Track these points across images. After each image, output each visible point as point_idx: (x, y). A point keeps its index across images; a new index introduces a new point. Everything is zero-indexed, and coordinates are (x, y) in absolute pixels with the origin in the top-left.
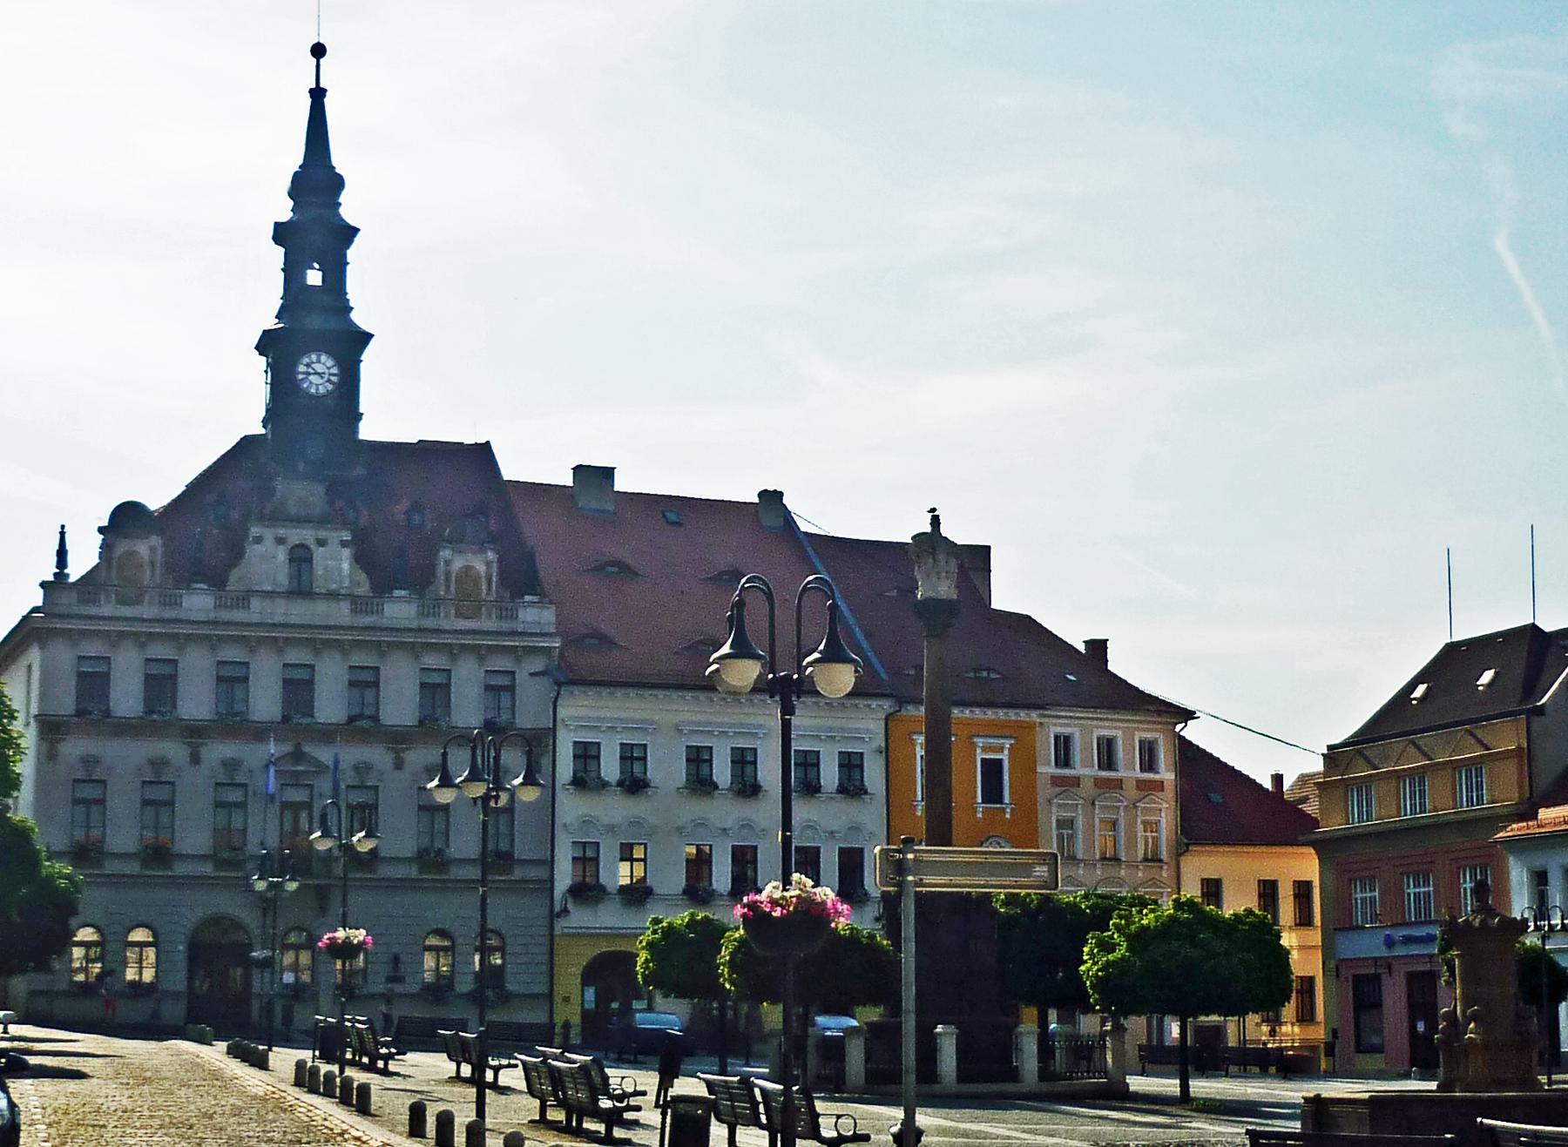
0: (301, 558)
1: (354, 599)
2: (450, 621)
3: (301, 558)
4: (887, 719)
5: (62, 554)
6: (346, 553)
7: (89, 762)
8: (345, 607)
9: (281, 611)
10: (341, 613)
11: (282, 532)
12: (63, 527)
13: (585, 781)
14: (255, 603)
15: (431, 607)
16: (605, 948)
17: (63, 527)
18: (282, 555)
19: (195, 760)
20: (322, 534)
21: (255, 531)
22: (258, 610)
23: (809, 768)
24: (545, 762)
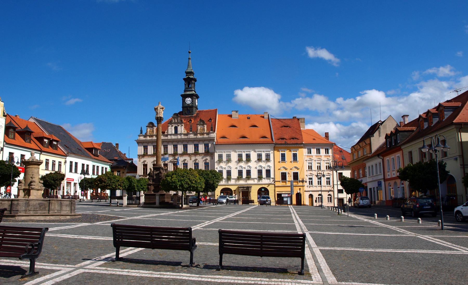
0: (176, 129)
1: (184, 134)
2: (199, 136)
3: (176, 129)
4: (274, 147)
5: (141, 132)
6: (183, 127)
7: (144, 161)
8: (183, 136)
9: (173, 137)
10: (183, 137)
11: (173, 125)
12: (141, 128)
13: (220, 160)
14: (169, 136)
15: (196, 134)
16: (224, 187)
17: (141, 128)
18: (173, 128)
20: (179, 124)
21: (169, 125)
22: (169, 137)
23: (268, 156)
24: (213, 157)
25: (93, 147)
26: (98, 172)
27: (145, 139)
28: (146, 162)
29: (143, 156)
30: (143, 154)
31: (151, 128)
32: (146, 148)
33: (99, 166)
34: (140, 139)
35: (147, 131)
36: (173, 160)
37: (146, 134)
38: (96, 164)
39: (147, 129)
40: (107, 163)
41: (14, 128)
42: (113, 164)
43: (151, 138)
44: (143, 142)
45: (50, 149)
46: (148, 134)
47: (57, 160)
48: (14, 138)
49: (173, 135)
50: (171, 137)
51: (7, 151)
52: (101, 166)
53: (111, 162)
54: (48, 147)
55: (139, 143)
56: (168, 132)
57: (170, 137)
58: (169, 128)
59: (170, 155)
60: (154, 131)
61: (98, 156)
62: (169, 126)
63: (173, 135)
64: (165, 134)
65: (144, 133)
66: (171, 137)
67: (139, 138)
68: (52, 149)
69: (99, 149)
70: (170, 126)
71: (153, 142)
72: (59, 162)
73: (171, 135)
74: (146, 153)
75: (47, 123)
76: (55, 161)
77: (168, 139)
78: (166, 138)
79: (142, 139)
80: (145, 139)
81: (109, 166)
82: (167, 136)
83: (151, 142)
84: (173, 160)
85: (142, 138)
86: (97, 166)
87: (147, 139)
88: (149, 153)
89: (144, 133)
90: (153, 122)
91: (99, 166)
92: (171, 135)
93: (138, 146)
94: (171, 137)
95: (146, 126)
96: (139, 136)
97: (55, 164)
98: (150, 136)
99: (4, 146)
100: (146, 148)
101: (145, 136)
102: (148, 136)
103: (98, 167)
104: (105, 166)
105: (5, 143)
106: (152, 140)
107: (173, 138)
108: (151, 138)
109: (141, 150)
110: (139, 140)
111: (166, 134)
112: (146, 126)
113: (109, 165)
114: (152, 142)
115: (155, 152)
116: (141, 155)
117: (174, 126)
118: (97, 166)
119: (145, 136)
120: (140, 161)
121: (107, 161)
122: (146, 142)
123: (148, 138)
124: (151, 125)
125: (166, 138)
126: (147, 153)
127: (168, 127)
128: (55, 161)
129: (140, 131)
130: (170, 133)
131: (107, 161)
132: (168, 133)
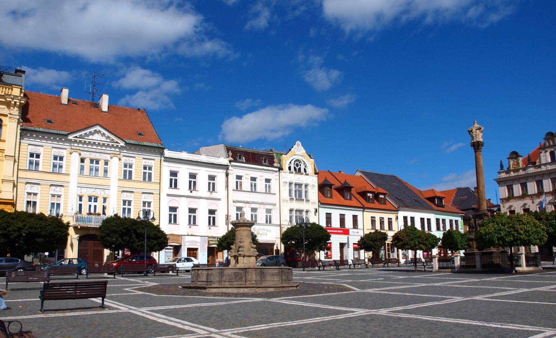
12: (501, 161)
17: (501, 161)
19: (533, 203)
22: (543, 168)
25: (435, 196)
26: (444, 227)
27: (508, 175)
28: (513, 207)
29: (508, 199)
30: (508, 197)
31: (514, 160)
32: (510, 189)
33: (445, 219)
34: (501, 177)
35: (509, 165)
36: (554, 200)
37: (508, 168)
38: (441, 217)
39: (509, 162)
40: (457, 214)
41: (330, 186)
42: (465, 214)
43: (516, 174)
44: (505, 180)
45: (376, 204)
46: (512, 169)
47: (386, 216)
48: (331, 197)
49: (549, 164)
50: (545, 167)
51: (323, 212)
52: (448, 218)
53: (463, 212)
54: (373, 203)
55: (500, 182)
56: (540, 162)
57: (544, 167)
58: (542, 154)
59: (547, 193)
60: (519, 163)
61: (443, 207)
62: (541, 152)
63: (549, 164)
64: (536, 164)
65: (505, 168)
66: (546, 168)
67: (499, 175)
68: (379, 204)
69: (444, 198)
70: (543, 152)
71: (519, 178)
72: (389, 219)
73: (545, 164)
74: (511, 194)
75: (377, 174)
76: (383, 218)
77: (541, 171)
78: (539, 170)
79: (503, 177)
80: (508, 175)
81: (460, 218)
82: (539, 167)
83: (516, 179)
84: (554, 200)
85: (503, 175)
86: (442, 219)
87: (510, 175)
88: (515, 195)
89: (505, 168)
90: (517, 151)
91: (445, 219)
92: (545, 164)
93: (500, 187)
94: (546, 168)
95: (508, 158)
96: (499, 173)
97: (383, 222)
98: (514, 171)
99: (319, 207)
100: (510, 189)
101: (508, 172)
102: (511, 171)
103: (444, 221)
104: (454, 218)
105: (319, 203)
106: (518, 175)
107: (550, 168)
108: (516, 174)
109: (504, 192)
110: (500, 178)
111: (537, 164)
112: (508, 158)
113: (461, 217)
114: (518, 179)
115: (524, 192)
116: (505, 199)
117: (549, 151)
118: (442, 219)
119: (508, 172)
120: (504, 207)
121: (457, 212)
122: (510, 180)
123: (512, 174)
124: (514, 156)
125: (539, 170)
126: (513, 195)
127: (540, 154)
128: (383, 218)
129: (500, 167)
130: (543, 162)
131: (458, 211)
132: (541, 163)
